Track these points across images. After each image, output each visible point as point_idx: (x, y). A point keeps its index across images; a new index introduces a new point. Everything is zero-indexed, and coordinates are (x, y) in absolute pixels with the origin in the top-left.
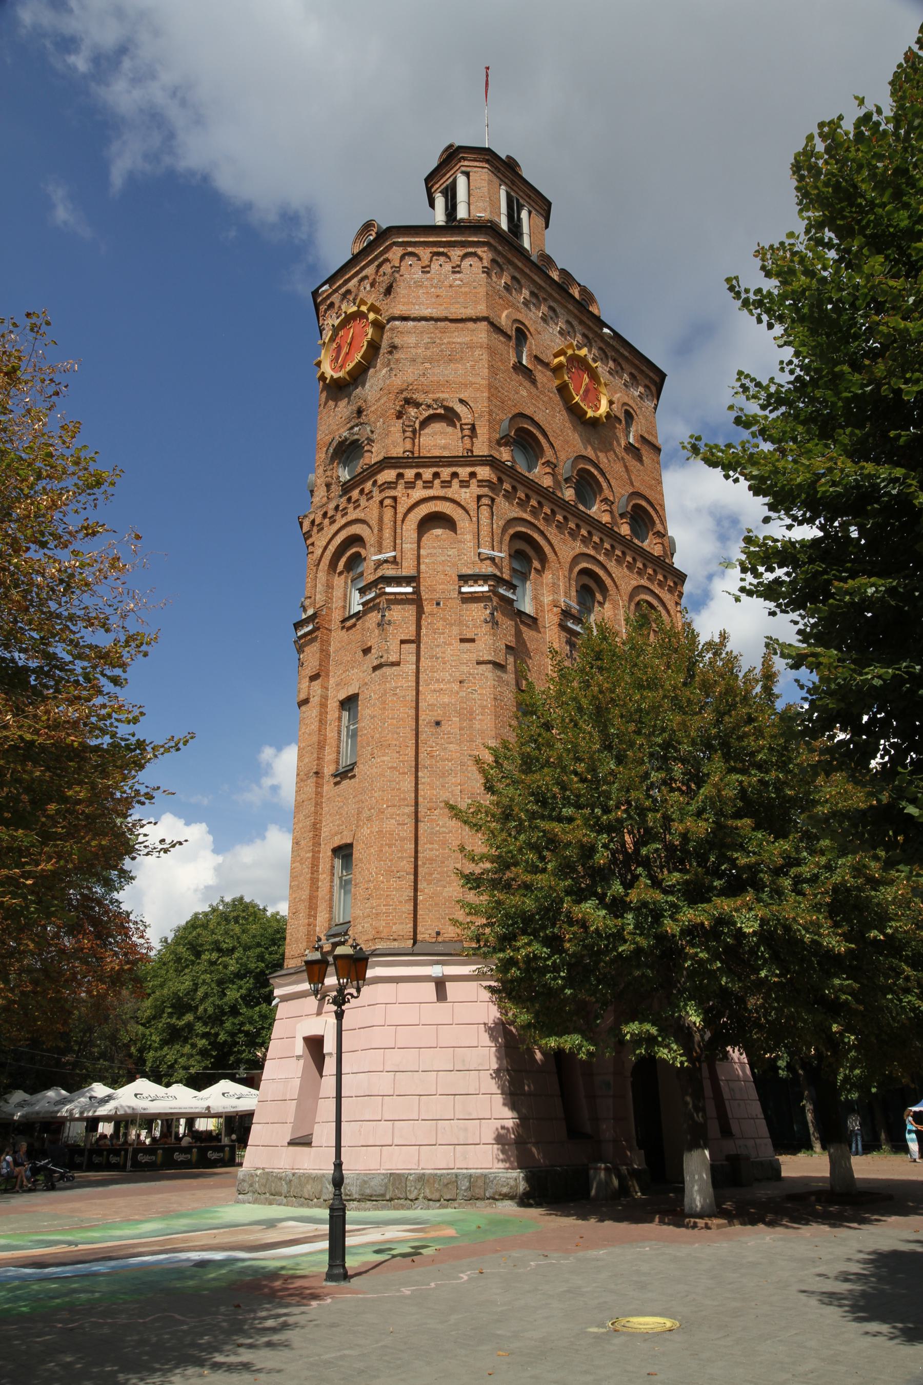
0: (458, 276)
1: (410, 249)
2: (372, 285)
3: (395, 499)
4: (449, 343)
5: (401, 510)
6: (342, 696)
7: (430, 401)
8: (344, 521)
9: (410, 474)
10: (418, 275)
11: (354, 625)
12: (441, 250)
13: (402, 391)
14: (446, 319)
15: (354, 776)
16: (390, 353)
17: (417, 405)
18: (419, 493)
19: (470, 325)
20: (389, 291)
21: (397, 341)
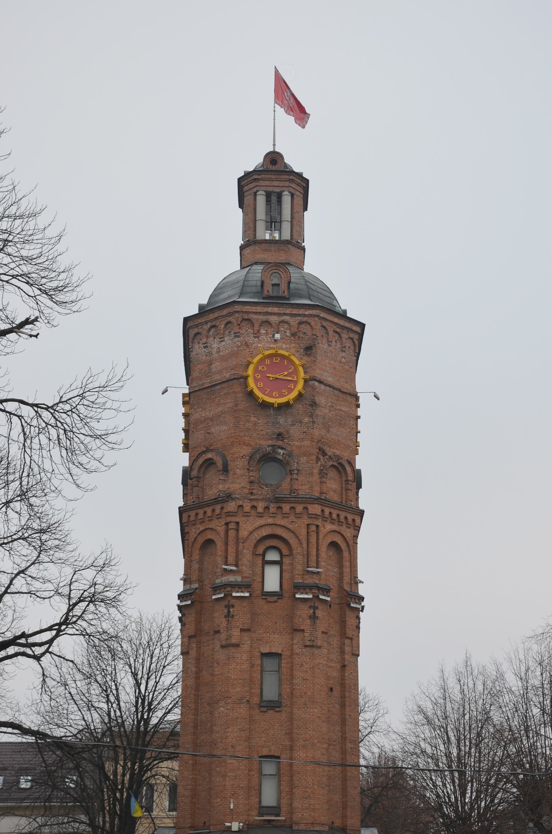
0: (344, 354)
1: (324, 324)
2: (293, 335)
3: (317, 526)
4: (340, 410)
5: (321, 537)
6: (266, 650)
7: (330, 454)
8: (270, 521)
9: (327, 511)
10: (326, 346)
11: (276, 602)
12: (338, 330)
13: (319, 441)
14: (340, 390)
15: (281, 711)
16: (311, 405)
17: (324, 454)
19: (349, 396)
20: (309, 349)
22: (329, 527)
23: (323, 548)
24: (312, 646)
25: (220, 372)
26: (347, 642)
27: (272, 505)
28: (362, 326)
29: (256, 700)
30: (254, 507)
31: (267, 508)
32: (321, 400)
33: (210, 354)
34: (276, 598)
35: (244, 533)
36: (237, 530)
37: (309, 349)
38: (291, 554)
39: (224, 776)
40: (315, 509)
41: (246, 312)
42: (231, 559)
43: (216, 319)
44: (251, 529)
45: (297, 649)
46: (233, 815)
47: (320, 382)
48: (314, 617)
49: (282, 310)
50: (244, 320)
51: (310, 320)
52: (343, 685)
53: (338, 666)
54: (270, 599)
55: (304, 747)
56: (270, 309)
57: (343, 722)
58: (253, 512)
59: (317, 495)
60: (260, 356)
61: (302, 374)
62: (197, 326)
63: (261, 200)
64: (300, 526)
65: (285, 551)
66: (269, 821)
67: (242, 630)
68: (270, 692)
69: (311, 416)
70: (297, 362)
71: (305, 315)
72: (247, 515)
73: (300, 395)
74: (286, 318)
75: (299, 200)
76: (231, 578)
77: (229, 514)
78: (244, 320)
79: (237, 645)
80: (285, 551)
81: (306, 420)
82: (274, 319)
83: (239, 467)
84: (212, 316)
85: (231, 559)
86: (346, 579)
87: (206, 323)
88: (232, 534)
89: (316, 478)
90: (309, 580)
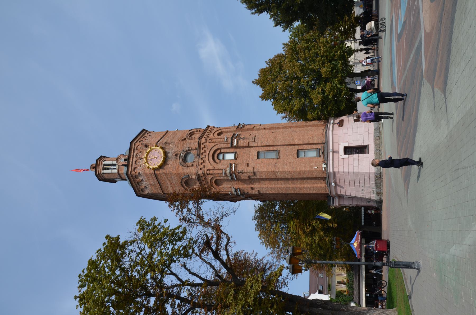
2: (141, 152)
5: (214, 138)
6: (256, 157)
8: (207, 157)
9: (205, 136)
17: (185, 139)
18: (211, 136)
21: (164, 142)
22: (211, 136)
23: (219, 137)
24: (255, 138)
25: (154, 181)
26: (255, 128)
27: (201, 157)
28: (144, 130)
29: (275, 161)
30: (201, 164)
31: (202, 159)
32: (165, 141)
33: (148, 185)
34: (236, 154)
35: (211, 168)
36: (210, 170)
37: (146, 146)
38: (220, 149)
39: (305, 171)
40: (203, 140)
41: (131, 169)
42: (220, 172)
43: (135, 183)
44: (209, 165)
45: (255, 144)
46: (320, 167)
47: (159, 141)
48: (244, 138)
49: (132, 156)
50: (134, 171)
51: (136, 146)
52: (271, 128)
53: (264, 131)
54: (237, 157)
55: (293, 140)
56: (131, 161)
57: (285, 128)
58: (203, 164)
59: (198, 140)
60: (146, 164)
61: (154, 147)
62: (139, 191)
63: (105, 171)
64: (209, 145)
65: (219, 151)
66: (323, 153)
67: (248, 166)
68: (273, 155)
69: (170, 144)
70: (150, 149)
71: (134, 148)
72: (204, 167)
73: (162, 148)
74: (135, 155)
75: (107, 159)
76: (228, 172)
77: (204, 174)
78: (134, 171)
79: (254, 168)
80: (219, 151)
81: (171, 145)
82: (134, 160)
83: (186, 170)
84: (134, 184)
85: (220, 172)
86: (232, 129)
87: (137, 187)
88: (211, 172)
89: (192, 141)
90: (230, 141)
